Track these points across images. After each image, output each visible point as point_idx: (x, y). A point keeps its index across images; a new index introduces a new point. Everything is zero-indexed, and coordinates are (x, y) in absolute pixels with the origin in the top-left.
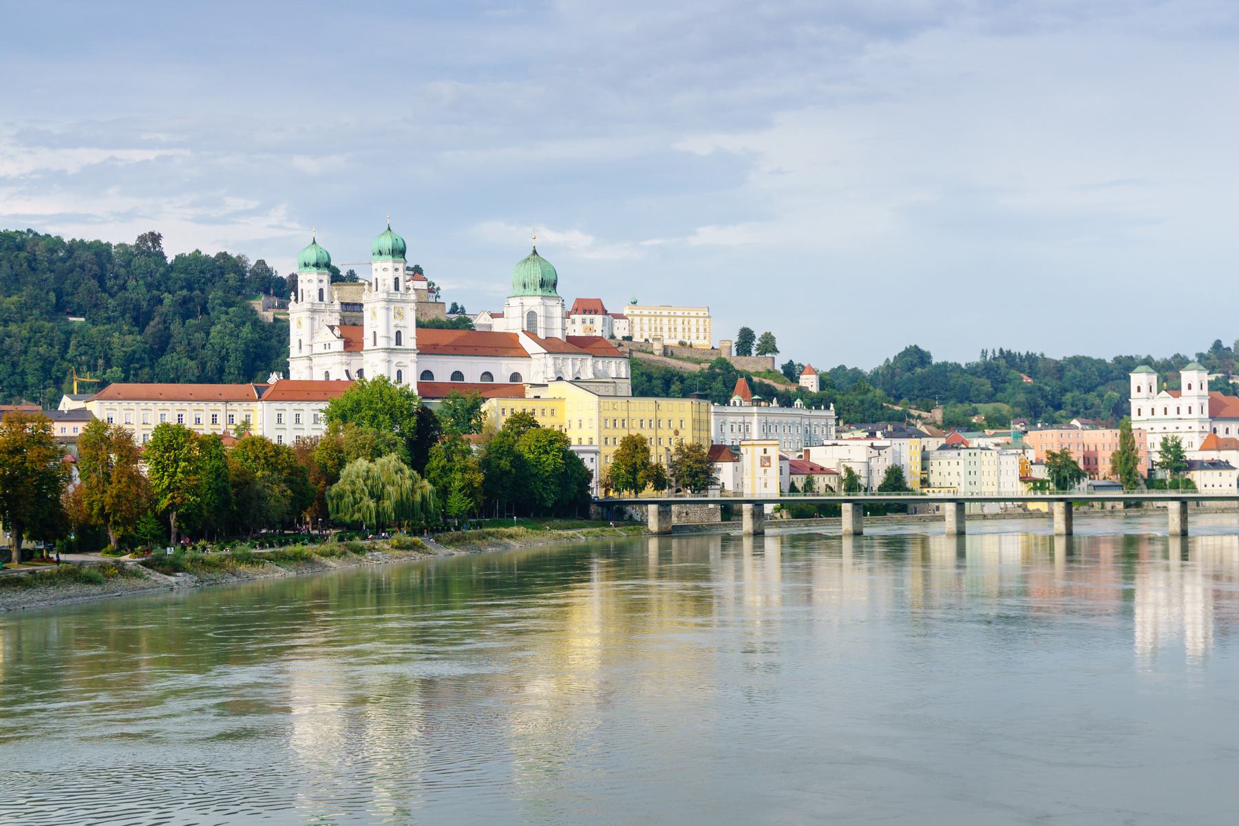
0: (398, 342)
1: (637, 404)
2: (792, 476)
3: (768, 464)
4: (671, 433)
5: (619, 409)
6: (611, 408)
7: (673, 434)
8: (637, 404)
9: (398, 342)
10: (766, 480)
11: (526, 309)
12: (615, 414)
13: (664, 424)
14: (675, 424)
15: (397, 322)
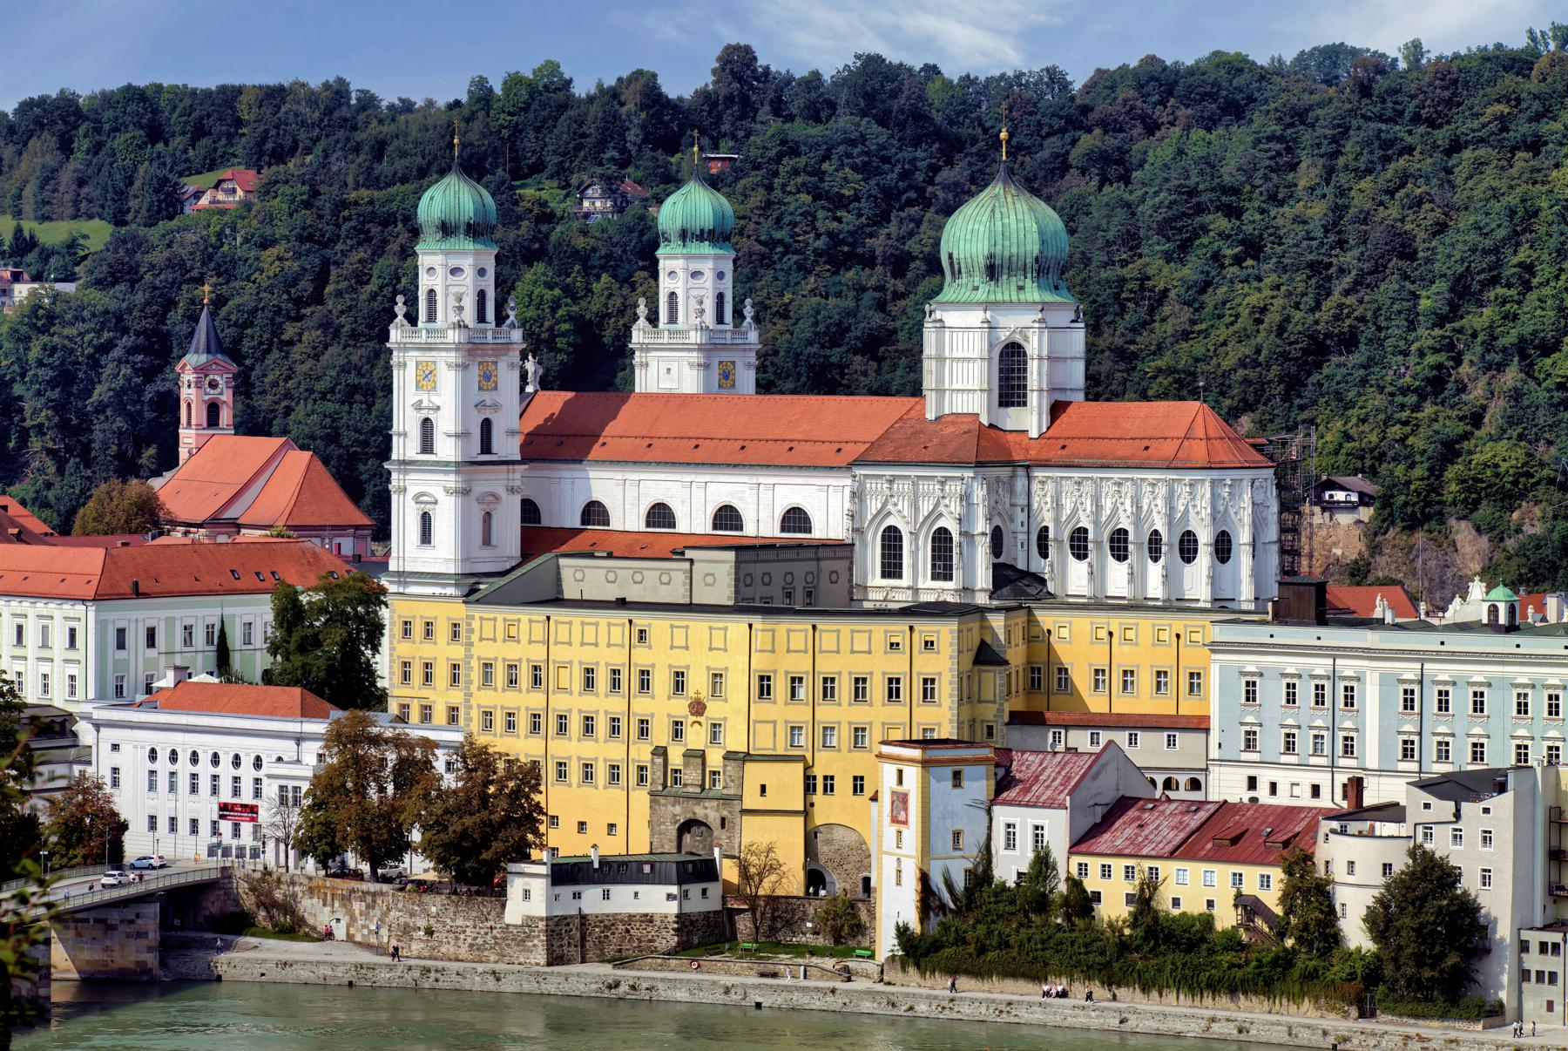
0: (486, 447)
4: (680, 707)
5: (524, 637)
6: (500, 635)
7: (686, 711)
9: (486, 447)
11: (1003, 336)
12: (512, 652)
13: (662, 681)
14: (697, 683)
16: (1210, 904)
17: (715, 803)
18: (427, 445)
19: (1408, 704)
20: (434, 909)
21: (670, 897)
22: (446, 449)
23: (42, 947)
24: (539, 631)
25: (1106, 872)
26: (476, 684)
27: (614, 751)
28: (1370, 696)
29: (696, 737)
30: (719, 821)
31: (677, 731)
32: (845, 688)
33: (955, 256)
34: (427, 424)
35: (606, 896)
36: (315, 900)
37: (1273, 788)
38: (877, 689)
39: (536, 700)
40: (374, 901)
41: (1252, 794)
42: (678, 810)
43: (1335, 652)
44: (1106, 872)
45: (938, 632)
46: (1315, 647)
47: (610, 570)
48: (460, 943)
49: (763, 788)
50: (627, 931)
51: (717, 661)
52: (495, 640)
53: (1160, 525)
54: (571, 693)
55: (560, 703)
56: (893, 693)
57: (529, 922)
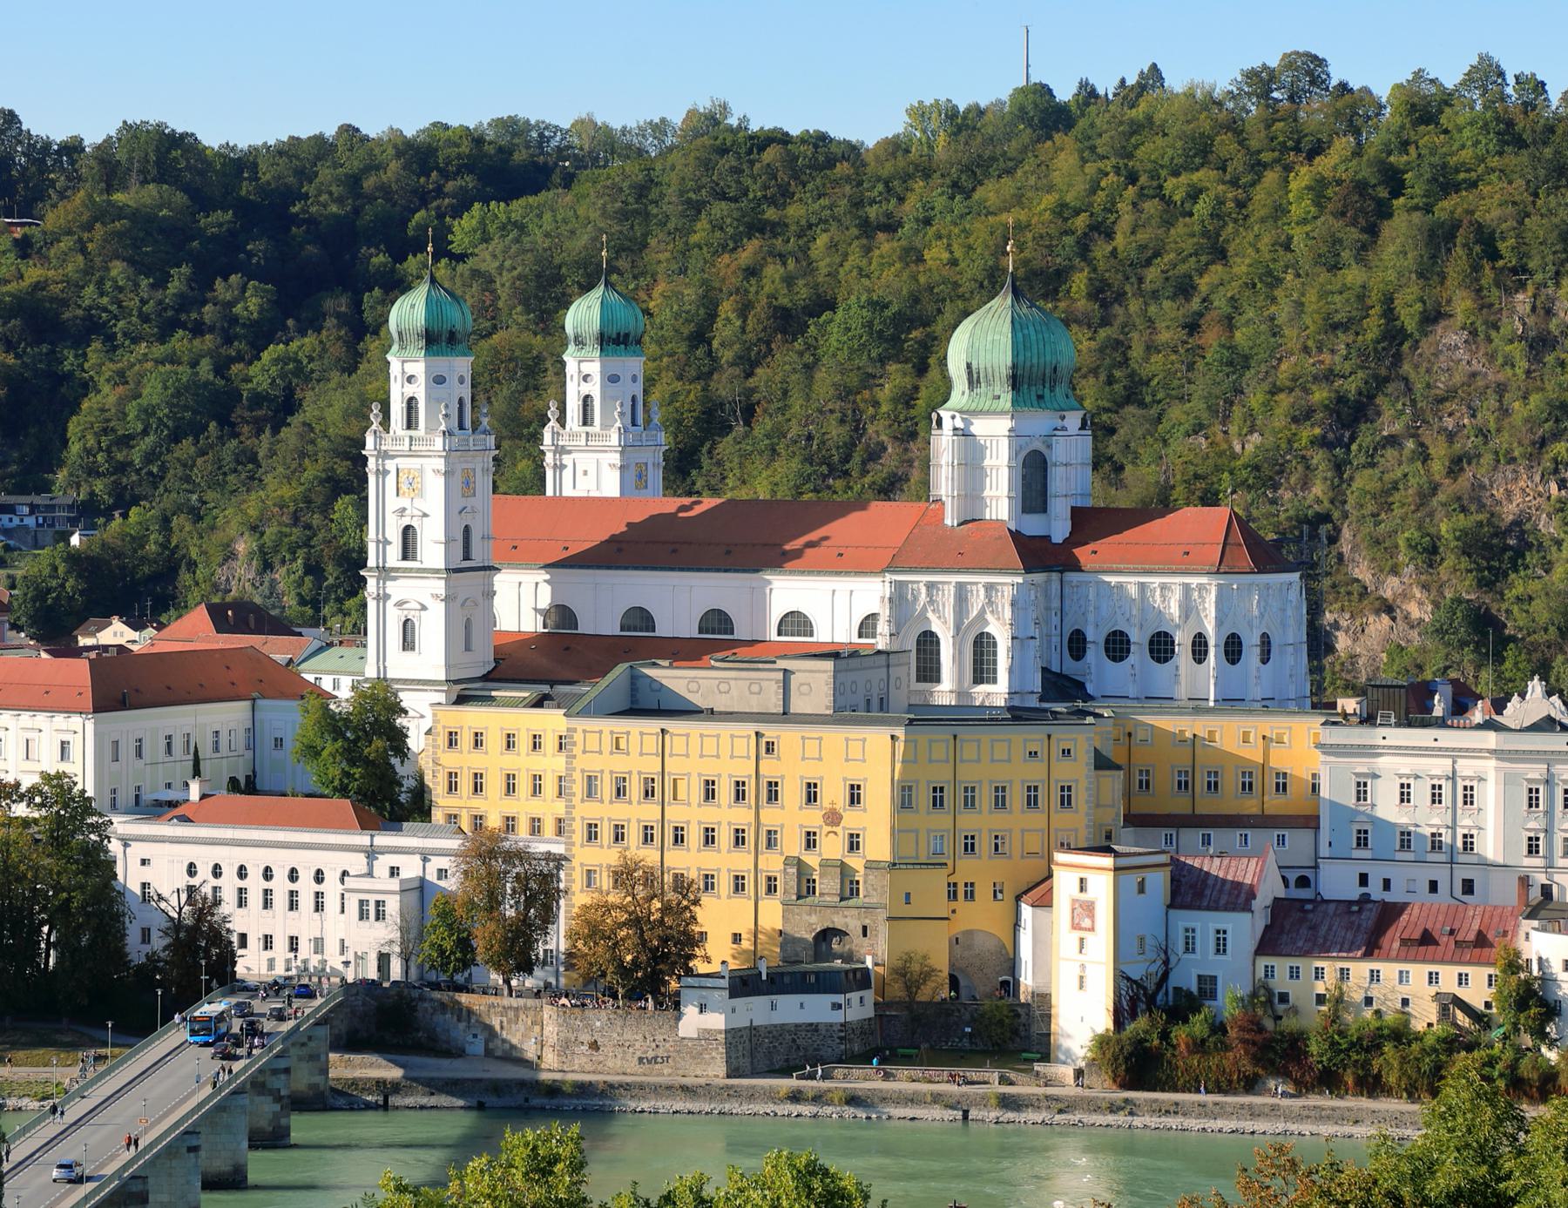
1: (695, 740)
2: (1263, 962)
3: (1087, 923)
5: (634, 748)
7: (820, 821)
8: (695, 740)
10: (1083, 966)
12: (620, 764)
13: (792, 793)
14: (833, 794)
15: (404, 502)
16: (1405, 1002)
17: (855, 912)
18: (408, 551)
19: (1533, 802)
20: (598, 1024)
21: (837, 1006)
22: (432, 552)
23: (283, 1077)
24: (652, 744)
25: (1294, 973)
26: (579, 796)
27: (742, 861)
28: (1490, 796)
29: (832, 847)
30: (860, 931)
31: (810, 842)
32: (985, 797)
33: (974, 366)
34: (408, 533)
35: (773, 1007)
36: (448, 1016)
37: (1387, 884)
38: (1017, 797)
39: (650, 812)
40: (517, 1017)
41: (1364, 890)
42: (814, 919)
43: (1454, 754)
44: (1294, 973)
45: (1075, 740)
46: (1433, 749)
47: (752, 681)
48: (629, 1056)
49: (908, 895)
50: (794, 1041)
51: (855, 774)
52: (600, 752)
53: (1210, 629)
54: (689, 804)
55: (675, 815)
56: (1032, 802)
57: (706, 1035)
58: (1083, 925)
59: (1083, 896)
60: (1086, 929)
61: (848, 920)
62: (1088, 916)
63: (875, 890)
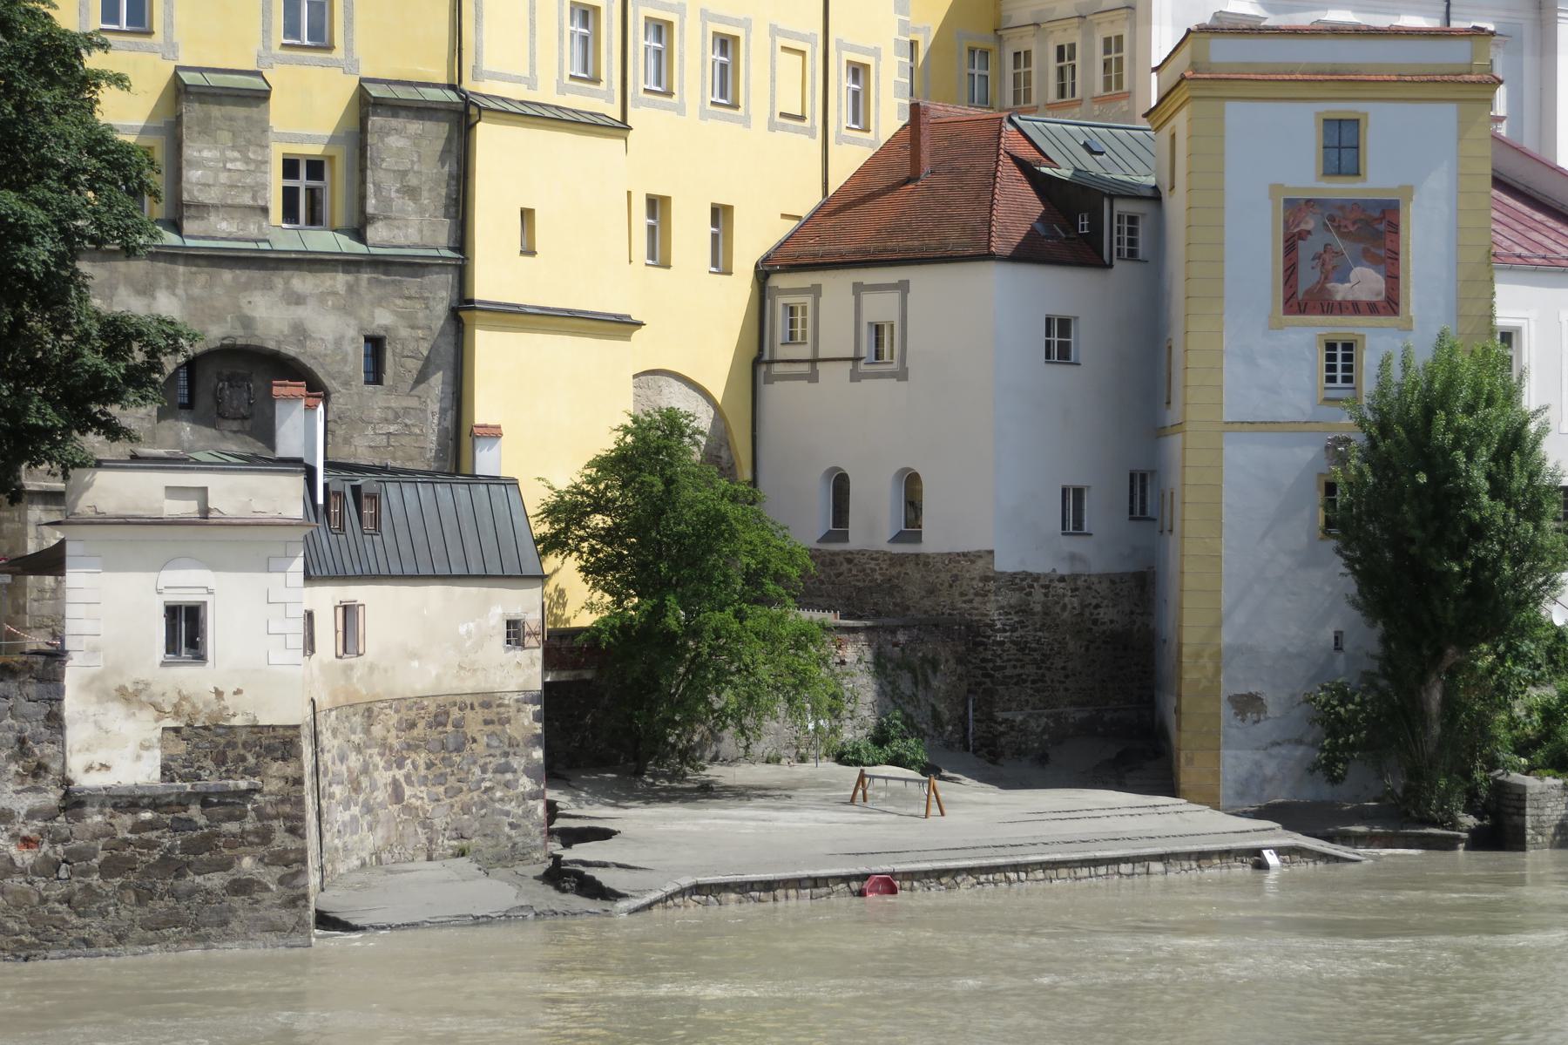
3: (1365, 282)
30: (356, 355)
58: (1341, 291)
59: (1342, 189)
60: (1355, 308)
61: (305, 313)
62: (1373, 260)
63: (411, 192)
